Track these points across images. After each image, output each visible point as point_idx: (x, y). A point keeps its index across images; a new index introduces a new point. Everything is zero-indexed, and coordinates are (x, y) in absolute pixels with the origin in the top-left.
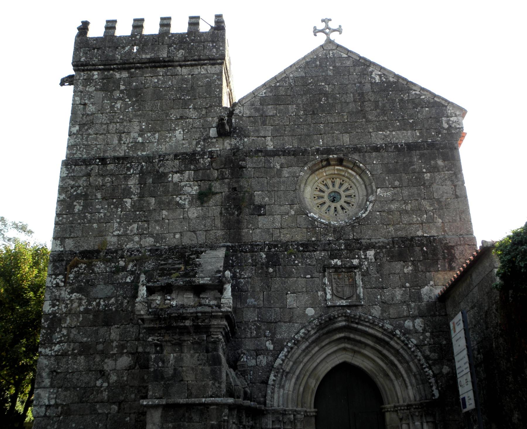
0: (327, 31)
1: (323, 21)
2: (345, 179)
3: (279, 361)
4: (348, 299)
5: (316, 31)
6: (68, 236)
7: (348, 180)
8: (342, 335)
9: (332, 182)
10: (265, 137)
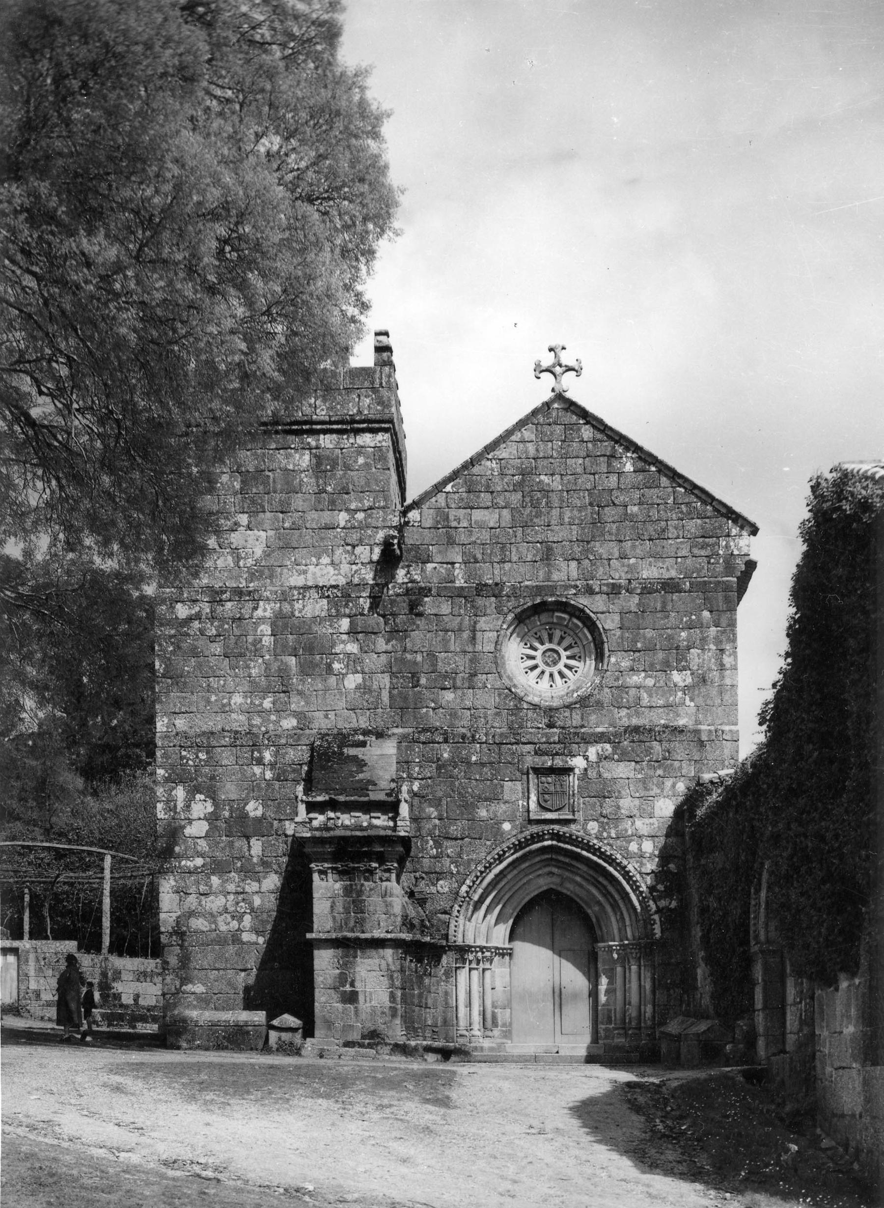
0: (558, 370)
1: (551, 350)
2: (568, 631)
3: (464, 888)
4: (556, 811)
5: (539, 370)
6: (177, 710)
7: (572, 633)
8: (549, 856)
9: (549, 634)
10: (453, 563)
